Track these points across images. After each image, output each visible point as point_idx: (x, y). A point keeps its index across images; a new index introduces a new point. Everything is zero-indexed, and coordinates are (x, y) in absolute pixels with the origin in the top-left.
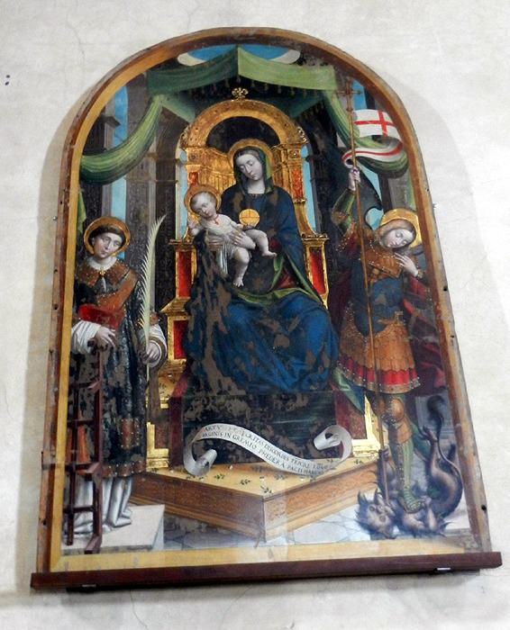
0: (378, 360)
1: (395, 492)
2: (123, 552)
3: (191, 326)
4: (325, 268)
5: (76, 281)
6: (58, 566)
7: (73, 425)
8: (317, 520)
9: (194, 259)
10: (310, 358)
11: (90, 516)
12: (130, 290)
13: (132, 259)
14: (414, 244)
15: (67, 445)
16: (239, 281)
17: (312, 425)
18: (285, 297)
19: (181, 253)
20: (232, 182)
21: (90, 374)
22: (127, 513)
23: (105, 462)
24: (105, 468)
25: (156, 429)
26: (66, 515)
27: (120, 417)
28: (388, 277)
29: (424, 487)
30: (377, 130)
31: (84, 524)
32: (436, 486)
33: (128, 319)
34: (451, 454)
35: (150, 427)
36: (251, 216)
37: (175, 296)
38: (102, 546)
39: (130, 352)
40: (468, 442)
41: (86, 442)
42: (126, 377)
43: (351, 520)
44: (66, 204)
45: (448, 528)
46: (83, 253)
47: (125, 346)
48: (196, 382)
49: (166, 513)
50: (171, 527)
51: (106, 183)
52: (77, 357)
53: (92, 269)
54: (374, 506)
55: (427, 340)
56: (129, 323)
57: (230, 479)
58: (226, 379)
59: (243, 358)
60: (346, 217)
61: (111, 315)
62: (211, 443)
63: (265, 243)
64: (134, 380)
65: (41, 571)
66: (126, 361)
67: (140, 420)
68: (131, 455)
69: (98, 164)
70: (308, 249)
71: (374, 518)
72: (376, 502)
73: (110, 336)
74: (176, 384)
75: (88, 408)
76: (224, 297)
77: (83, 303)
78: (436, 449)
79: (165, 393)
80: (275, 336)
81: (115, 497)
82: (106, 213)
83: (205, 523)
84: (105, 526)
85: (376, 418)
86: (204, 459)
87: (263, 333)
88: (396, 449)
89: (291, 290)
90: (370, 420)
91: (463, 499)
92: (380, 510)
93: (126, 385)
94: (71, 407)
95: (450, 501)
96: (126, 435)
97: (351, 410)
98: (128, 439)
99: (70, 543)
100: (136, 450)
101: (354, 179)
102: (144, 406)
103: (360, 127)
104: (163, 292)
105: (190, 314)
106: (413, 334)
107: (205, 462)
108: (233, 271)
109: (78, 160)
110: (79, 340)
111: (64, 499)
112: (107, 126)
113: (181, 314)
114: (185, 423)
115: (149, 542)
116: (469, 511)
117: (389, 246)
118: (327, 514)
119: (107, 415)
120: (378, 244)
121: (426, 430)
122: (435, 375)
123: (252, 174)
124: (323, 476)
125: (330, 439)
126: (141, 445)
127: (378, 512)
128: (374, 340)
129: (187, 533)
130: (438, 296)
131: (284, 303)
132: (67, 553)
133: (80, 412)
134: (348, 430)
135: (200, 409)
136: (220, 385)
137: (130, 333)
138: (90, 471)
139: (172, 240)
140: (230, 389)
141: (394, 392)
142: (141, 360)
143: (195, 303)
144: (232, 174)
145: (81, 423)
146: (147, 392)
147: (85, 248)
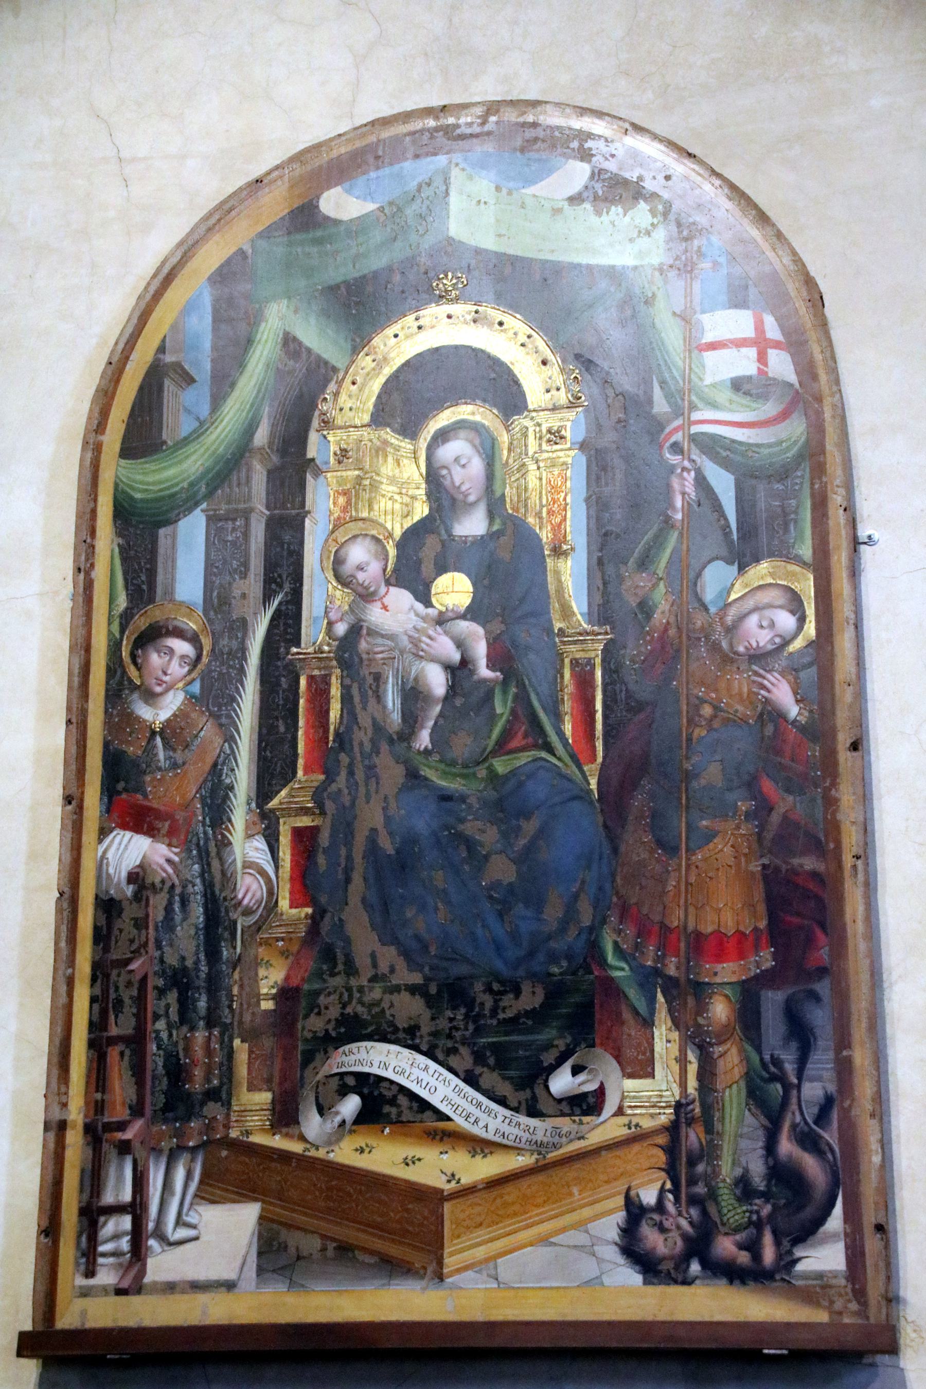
0: (691, 910)
1: (700, 1189)
2: (183, 1292)
3: (324, 839)
4: (599, 706)
5: (106, 745)
6: (66, 1320)
7: (98, 1045)
8: (544, 1240)
9: (335, 691)
10: (553, 913)
11: (126, 1222)
12: (209, 761)
13: (215, 696)
14: (798, 644)
15: (88, 1083)
16: (424, 739)
18: (513, 773)
19: (311, 679)
20: (421, 510)
21: (132, 941)
22: (192, 1218)
23: (153, 1120)
24: (155, 1129)
25: (251, 1052)
26: (84, 1219)
27: (185, 1029)
29: (759, 1182)
30: (744, 363)
31: (116, 1237)
32: (784, 1176)
33: (204, 825)
34: (822, 1117)
36: (454, 589)
37: (295, 773)
38: (148, 1279)
39: (205, 895)
40: (864, 1088)
41: (121, 1078)
42: (198, 946)
43: (608, 1243)
44: (88, 573)
46: (120, 683)
47: (198, 881)
48: (328, 955)
49: (262, 1219)
50: (271, 1245)
52: (108, 906)
53: (138, 719)
54: (656, 1217)
55: (801, 866)
56: (205, 833)
57: (385, 1156)
58: (385, 949)
59: (423, 908)
60: (655, 586)
61: (169, 816)
62: (351, 1081)
63: (480, 650)
64: (213, 954)
65: (40, 1328)
66: (198, 912)
67: (222, 1034)
68: (203, 1104)
69: (153, 477)
70: (567, 661)
72: (660, 1207)
73: (169, 861)
74: (289, 961)
75: (126, 1010)
76: (391, 774)
77: (119, 793)
78: (794, 1100)
79: (271, 978)
80: (486, 858)
81: (172, 1184)
83: (333, 1240)
84: (152, 1242)
85: (675, 1035)
86: (337, 1113)
87: (464, 854)
88: (710, 1100)
89: (524, 758)
90: (664, 1040)
91: (838, 1209)
92: (667, 1224)
93: (197, 962)
94: (96, 1006)
95: (809, 1212)
96: (194, 1063)
97: (627, 1015)
98: (198, 1072)
99: (90, 1273)
100: (212, 1095)
101: (684, 487)
102: (230, 1007)
103: (710, 357)
104: (273, 770)
105: (323, 813)
106: (770, 852)
107: (338, 1119)
108: (411, 720)
109: (112, 468)
110: (111, 871)
111: (81, 1191)
113: (305, 811)
114: (306, 1040)
115: (230, 1274)
116: (846, 1235)
117: (741, 649)
118: (564, 1230)
119: (161, 1025)
121: (777, 1062)
122: (810, 942)
123: (464, 488)
124: (561, 1151)
125: (582, 1077)
126: (222, 1084)
127: (662, 1229)
128: (688, 867)
129: (299, 1258)
130: (835, 764)
131: (510, 785)
132: (85, 1293)
133: (112, 1018)
134: (618, 1058)
135: (334, 1012)
136: (375, 965)
137: (208, 853)
138: (128, 1135)
139: (294, 650)
140: (392, 970)
141: (718, 980)
142: (227, 912)
143: (334, 787)
144: (422, 492)
145: (112, 1041)
146: (236, 976)
147: (124, 672)
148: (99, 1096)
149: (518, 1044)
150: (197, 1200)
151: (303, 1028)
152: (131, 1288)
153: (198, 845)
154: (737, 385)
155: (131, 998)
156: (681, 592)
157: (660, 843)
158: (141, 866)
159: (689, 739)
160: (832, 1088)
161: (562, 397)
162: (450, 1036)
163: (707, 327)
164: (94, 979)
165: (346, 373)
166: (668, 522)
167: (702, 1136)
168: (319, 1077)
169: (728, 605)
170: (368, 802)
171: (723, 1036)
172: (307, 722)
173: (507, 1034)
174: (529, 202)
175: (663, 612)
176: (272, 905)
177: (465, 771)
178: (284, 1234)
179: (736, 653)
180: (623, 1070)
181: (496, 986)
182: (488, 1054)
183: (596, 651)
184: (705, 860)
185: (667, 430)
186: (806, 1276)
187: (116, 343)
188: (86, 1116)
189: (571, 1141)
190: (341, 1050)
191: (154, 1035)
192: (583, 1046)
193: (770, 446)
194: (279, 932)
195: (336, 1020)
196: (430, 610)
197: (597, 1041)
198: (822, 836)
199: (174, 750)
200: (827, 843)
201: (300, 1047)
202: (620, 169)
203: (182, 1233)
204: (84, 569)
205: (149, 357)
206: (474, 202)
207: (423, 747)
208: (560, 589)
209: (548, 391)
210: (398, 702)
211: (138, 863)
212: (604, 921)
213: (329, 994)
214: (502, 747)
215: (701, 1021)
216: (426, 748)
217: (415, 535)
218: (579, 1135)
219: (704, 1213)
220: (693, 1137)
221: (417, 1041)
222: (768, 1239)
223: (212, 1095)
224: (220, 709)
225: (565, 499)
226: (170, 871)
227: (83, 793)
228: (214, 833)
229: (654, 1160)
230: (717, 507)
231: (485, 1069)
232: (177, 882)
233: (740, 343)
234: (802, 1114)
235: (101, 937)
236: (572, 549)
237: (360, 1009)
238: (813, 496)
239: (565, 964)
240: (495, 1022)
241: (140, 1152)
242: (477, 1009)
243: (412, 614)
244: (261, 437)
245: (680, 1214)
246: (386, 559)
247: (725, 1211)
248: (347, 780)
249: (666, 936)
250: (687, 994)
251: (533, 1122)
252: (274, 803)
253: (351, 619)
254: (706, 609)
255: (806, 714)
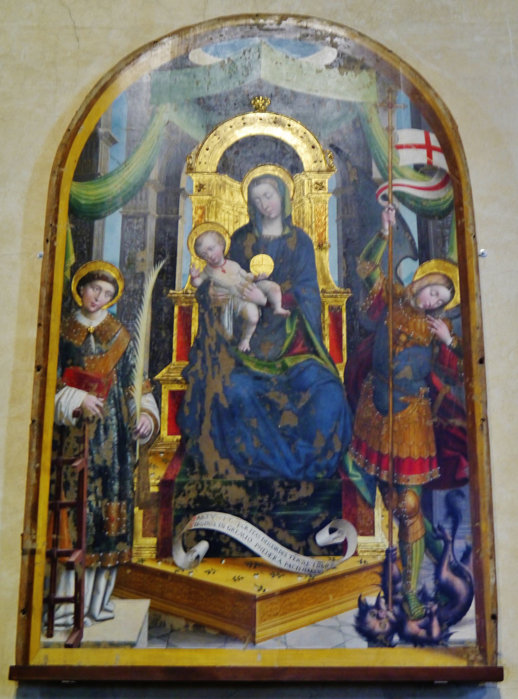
0: (395, 446)
1: (400, 597)
2: (105, 647)
3: (188, 398)
5: (61, 339)
6: (37, 659)
7: (55, 507)
8: (313, 623)
9: (195, 316)
10: (319, 443)
11: (71, 608)
12: (122, 351)
13: (126, 313)
14: (451, 305)
15: (48, 529)
16: (245, 345)
17: (316, 517)
18: (296, 366)
19: (181, 309)
20: (245, 220)
21: (75, 450)
22: (109, 607)
24: (88, 556)
25: (144, 515)
27: (106, 501)
28: (417, 345)
31: (65, 615)
32: (444, 590)
34: (465, 557)
35: (138, 513)
36: (263, 264)
38: (84, 640)
40: (486, 543)
41: (68, 527)
42: (114, 454)
44: (52, 243)
45: (452, 638)
46: (70, 304)
47: (114, 418)
48: (190, 463)
49: (151, 608)
51: (99, 217)
52: (61, 430)
53: (80, 325)
54: (375, 611)
57: (223, 576)
59: (244, 439)
60: (375, 269)
62: (203, 534)
63: (278, 298)
64: (123, 460)
65: (21, 664)
66: (114, 436)
67: (128, 504)
68: (116, 543)
69: (89, 193)
70: (327, 307)
71: (372, 623)
72: (377, 606)
73: (97, 406)
74: (168, 464)
75: (71, 488)
76: (227, 364)
77: (68, 366)
79: (156, 475)
80: (281, 412)
81: (99, 587)
82: (98, 256)
83: (192, 621)
84: (86, 620)
85: (386, 513)
86: (195, 551)
88: (405, 548)
89: (302, 359)
90: (380, 515)
92: (382, 615)
93: (113, 463)
94: (53, 486)
95: (457, 609)
96: (111, 520)
97: (360, 502)
98: (113, 526)
99: (50, 634)
100: (122, 538)
101: (389, 220)
102: (132, 489)
103: (402, 153)
104: (158, 358)
105: (187, 383)
106: (438, 414)
107: (195, 555)
108: (239, 333)
109: (68, 186)
110: (63, 409)
111: (45, 588)
112: (102, 145)
113: (178, 382)
114: (177, 510)
115: (132, 638)
116: (477, 621)
117: (421, 306)
118: (324, 618)
119: (92, 498)
120: (407, 304)
121: (440, 528)
122: (458, 465)
123: (269, 210)
125: (335, 535)
126: (127, 533)
127: (378, 618)
128: (393, 421)
129: (172, 630)
131: (296, 372)
132: (47, 646)
133: (63, 493)
135: (193, 495)
136: (217, 468)
138: (72, 559)
140: (227, 472)
142: (131, 435)
143: (193, 370)
144: (245, 210)
146: (136, 472)
147: (73, 298)
148: (55, 536)
149: (299, 517)
150: (113, 597)
151: (175, 503)
152: (75, 643)
153: (114, 397)
154: (417, 168)
155: (74, 482)
156: (389, 273)
157: (378, 408)
158: (81, 407)
159: (394, 353)
160: (470, 543)
161: (324, 166)
162: (260, 510)
163: (400, 136)
164: (52, 471)
165: (203, 144)
166: (381, 236)
167: (401, 567)
168: (185, 530)
169: (413, 283)
170: (213, 378)
171: (412, 514)
172: (179, 332)
173: (291, 510)
174: (305, 65)
175: (379, 284)
176: (157, 433)
177: (270, 364)
178: (164, 617)
179: (418, 308)
180: (358, 530)
181: (286, 484)
182: (282, 521)
183: (343, 302)
184: (402, 418)
185: (381, 187)
186: (456, 642)
187: (73, 120)
188: (47, 547)
189: (328, 570)
190: (197, 516)
191: (88, 503)
192: (335, 518)
193: (433, 200)
194: (161, 449)
195: (194, 499)
196: (249, 274)
197: (344, 515)
198: (465, 407)
199: (101, 343)
200: (468, 412)
201: (174, 513)
202: (353, 53)
203: (104, 615)
204: (50, 241)
205: (92, 128)
206: (274, 62)
207: (245, 350)
208: (323, 268)
209: (315, 162)
210: (231, 324)
211: (79, 405)
212: (347, 450)
213: (190, 485)
214: (290, 351)
215: (400, 506)
216: (247, 350)
217: (240, 235)
218: (333, 566)
219: (402, 610)
220: (395, 569)
221: (241, 512)
222: (435, 623)
223: (122, 538)
224: (128, 322)
225: (325, 219)
226: (98, 411)
227: (47, 365)
228: (124, 391)
229: (374, 581)
230: (407, 230)
231: (279, 529)
232: (101, 417)
233: (419, 147)
234: (454, 556)
235: (57, 447)
236: (329, 246)
237: (208, 494)
238: (458, 228)
239: (325, 473)
240: (285, 503)
241: (80, 569)
242: (275, 496)
243: (239, 276)
244: (154, 175)
245: (388, 610)
246: (225, 245)
247: (413, 608)
248: (202, 365)
249: (381, 459)
250: (392, 491)
251: (307, 559)
252: (158, 377)
253: (205, 277)
254: (402, 283)
255: (456, 342)
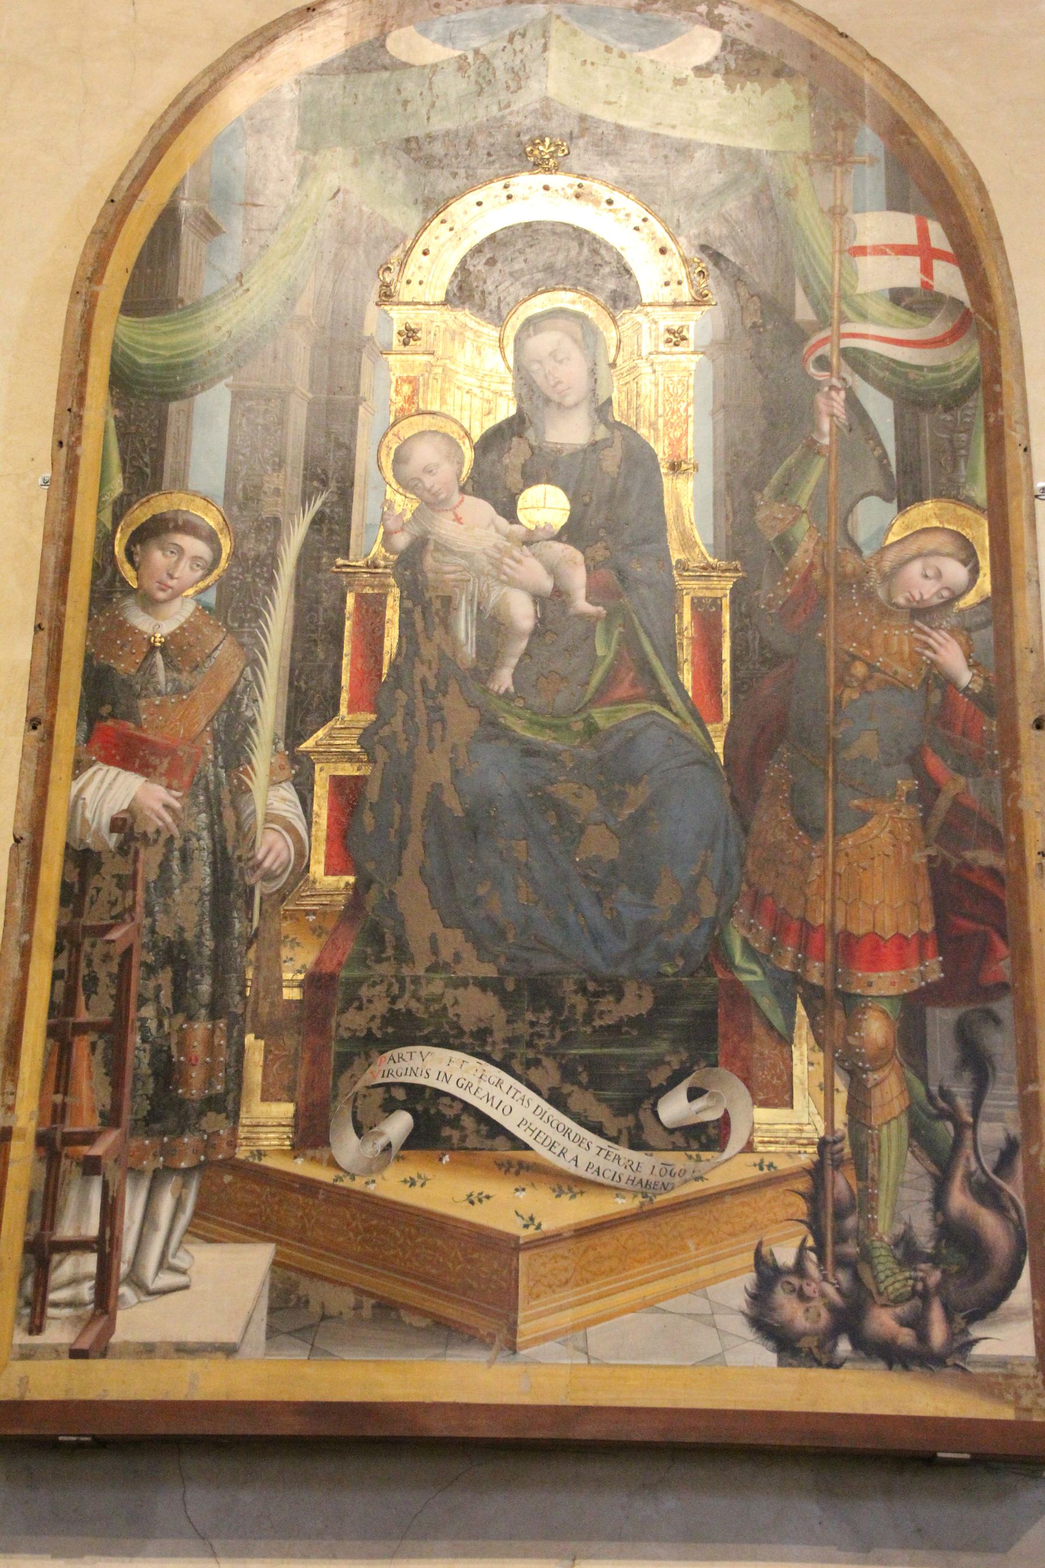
0: (839, 904)
1: (851, 1249)
3: (373, 793)
4: (726, 654)
5: (88, 659)
7: (61, 1033)
8: (649, 1305)
9: (392, 614)
10: (667, 899)
11: (90, 1263)
12: (225, 687)
14: (970, 599)
16: (504, 680)
17: (658, 1062)
18: (618, 728)
19: (360, 598)
20: (506, 409)
21: (114, 904)
23: (133, 1132)
24: (134, 1144)
25: (267, 1052)
26: (30, 1256)
27: (180, 1018)
28: (893, 685)
29: (925, 1242)
30: (906, 273)
31: (74, 1281)
32: (958, 1238)
33: (215, 765)
35: (254, 1046)
37: (336, 709)
38: (113, 1340)
39: (214, 852)
42: (202, 915)
43: (732, 1311)
44: (72, 448)
45: (978, 1350)
46: (111, 583)
47: (205, 834)
48: (375, 936)
50: (287, 1301)
51: (179, 395)
52: (82, 859)
53: (133, 630)
54: (795, 1281)
55: (975, 860)
56: (217, 775)
57: (443, 1190)
58: (449, 932)
61: (170, 751)
62: (400, 1095)
63: (578, 579)
64: (221, 926)
66: (203, 873)
67: (230, 1027)
68: (201, 1114)
70: (687, 600)
71: (790, 1310)
72: (799, 1269)
73: (167, 806)
74: (325, 938)
75: (101, 989)
76: (462, 720)
78: (969, 1143)
80: (582, 830)
81: (155, 1216)
82: (174, 480)
83: (371, 1295)
84: (124, 1290)
85: (820, 1056)
86: (381, 1134)
87: (554, 823)
88: (863, 1139)
89: (629, 713)
90: (805, 1061)
91: (1025, 1280)
92: (809, 1290)
93: (201, 934)
94: (60, 984)
95: (990, 1281)
96: (191, 1062)
97: (759, 1030)
98: (196, 1074)
99: (36, 1328)
100: (214, 1103)
101: (830, 411)
102: (242, 993)
105: (372, 760)
107: (382, 1142)
108: (490, 652)
109: (108, 326)
110: (88, 815)
111: (29, 1219)
112: (188, 237)
113: (351, 757)
114: (342, 1041)
116: (1035, 1313)
117: (901, 601)
118: (676, 1292)
119: (148, 1011)
120: (869, 596)
121: (946, 1095)
122: (987, 951)
124: (673, 1194)
125: (700, 1103)
126: (227, 1092)
127: (802, 1296)
129: (324, 1317)
130: (1016, 741)
132: (27, 1354)
133: (82, 999)
134: (745, 1080)
135: (380, 1007)
136: (435, 951)
137: (219, 802)
138: (97, 1150)
139: (340, 561)
140: (457, 957)
141: (873, 992)
143: (385, 731)
145: (81, 1029)
146: (251, 955)
147: (116, 571)
148: (58, 1098)
149: (618, 1059)
150: (190, 1237)
151: (338, 1026)
153: (206, 788)
154: (898, 296)
155: (110, 975)
156: (828, 528)
157: (801, 823)
158: (129, 810)
159: (838, 703)
160: (1016, 1130)
161: (686, 293)
162: (530, 1045)
163: (860, 227)
164: (58, 950)
165: (416, 240)
166: (812, 448)
167: (853, 1183)
168: (359, 1086)
169: (883, 550)
170: (431, 752)
171: (879, 1060)
172: (354, 648)
173: (602, 1046)
174: (647, 68)
175: (806, 551)
176: (301, 869)
177: (556, 721)
179: (897, 606)
180: (753, 1095)
181: (591, 986)
182: (580, 1069)
183: (723, 588)
184: (857, 846)
185: (814, 340)
186: (986, 1362)
187: (121, 178)
188: (39, 1124)
189: (686, 1181)
190: (388, 1054)
191: (138, 1024)
192: (703, 1064)
193: (931, 369)
194: (310, 904)
195: (383, 1017)
196: (515, 527)
197: (721, 1059)
198: (1000, 825)
199: (180, 671)
200: (1007, 835)
201: (334, 1047)
202: (758, 41)
203: (167, 1279)
204: (67, 443)
205: (165, 199)
206: (579, 62)
207: (502, 690)
208: (679, 515)
209: (667, 284)
210: (473, 633)
211: (125, 806)
212: (730, 913)
213: (374, 984)
214: (601, 696)
215: (851, 1040)
216: (507, 691)
217: (494, 441)
218: (696, 1175)
219: (856, 1278)
220: (842, 1183)
221: (488, 1048)
222: (936, 1314)
223: (214, 1103)
224: (241, 626)
225: (686, 410)
226: (169, 819)
227: (54, 716)
228: (228, 776)
229: (791, 1210)
230: (873, 435)
231: (575, 1088)
232: (176, 833)
233: (904, 250)
234: (978, 1159)
235: (71, 896)
236: (696, 467)
237: (414, 1005)
238: (987, 429)
239: (681, 962)
240: (589, 1030)
241: (113, 1174)
242: (566, 1013)
243: (492, 528)
244: (303, 307)
245: (825, 1278)
246: (461, 464)
247: (882, 1276)
248: (404, 723)
249: (806, 934)
251: (637, 1156)
252: (308, 744)
253: (416, 530)
254: (858, 551)
255: (981, 681)
